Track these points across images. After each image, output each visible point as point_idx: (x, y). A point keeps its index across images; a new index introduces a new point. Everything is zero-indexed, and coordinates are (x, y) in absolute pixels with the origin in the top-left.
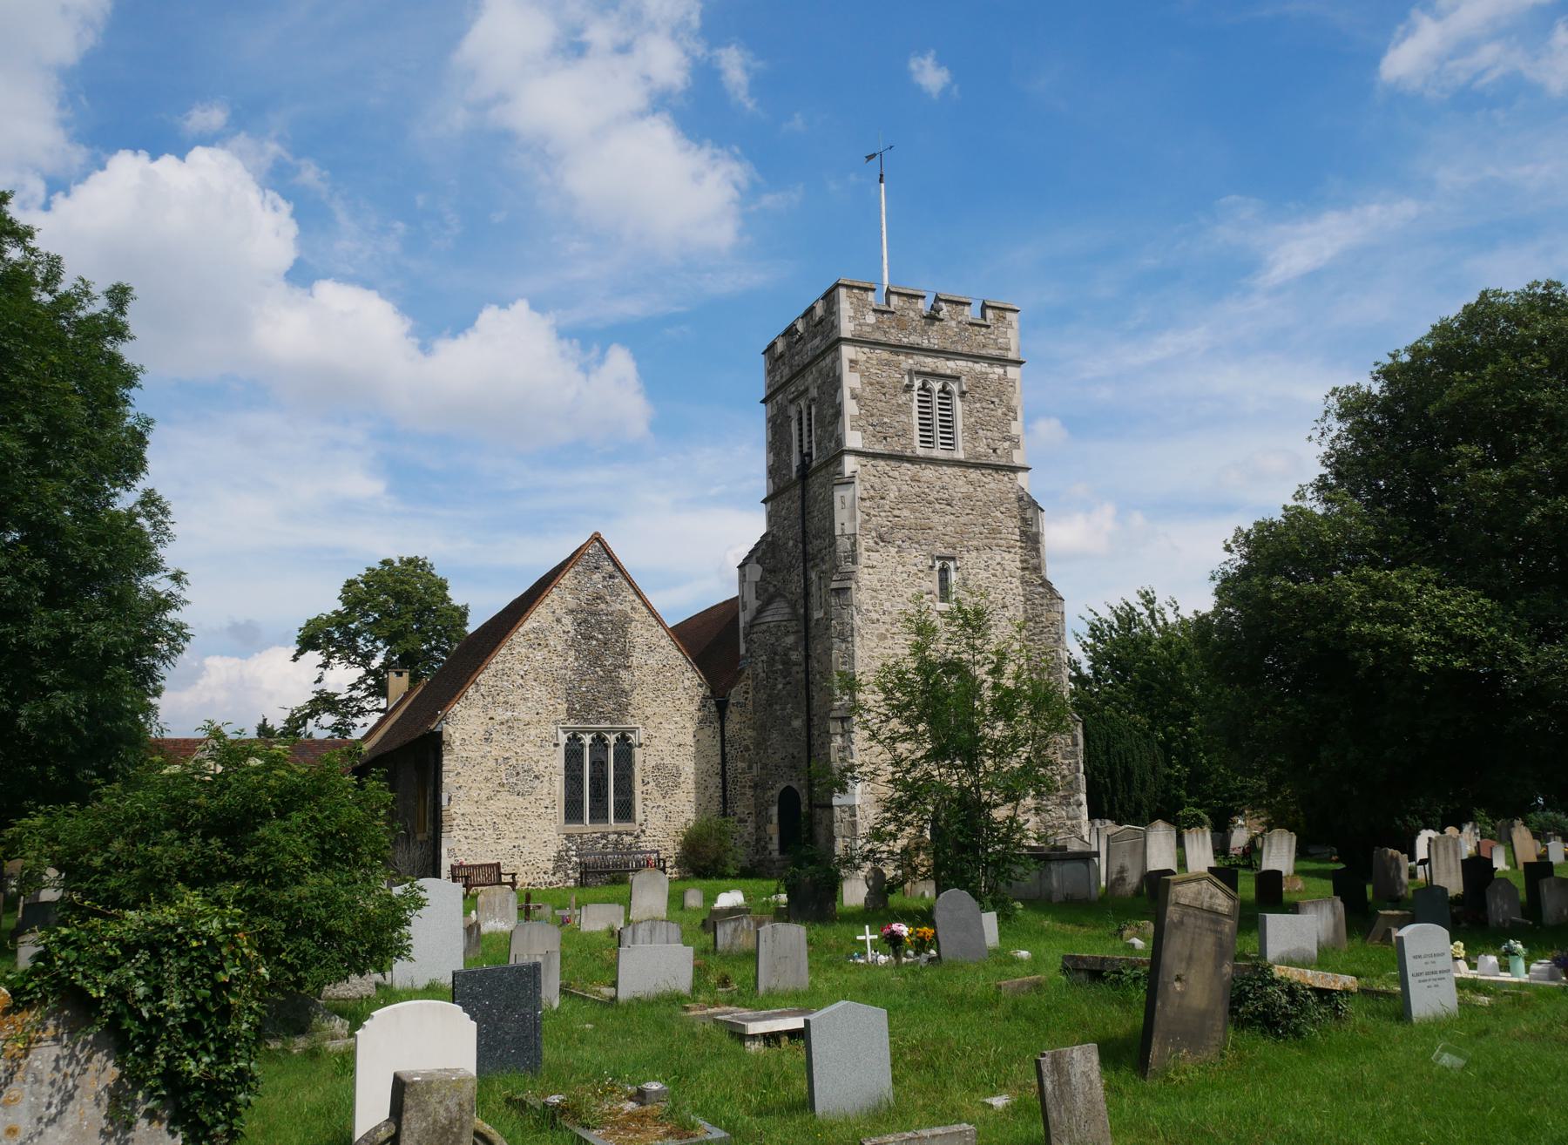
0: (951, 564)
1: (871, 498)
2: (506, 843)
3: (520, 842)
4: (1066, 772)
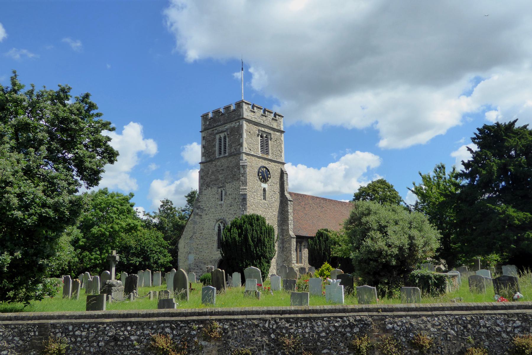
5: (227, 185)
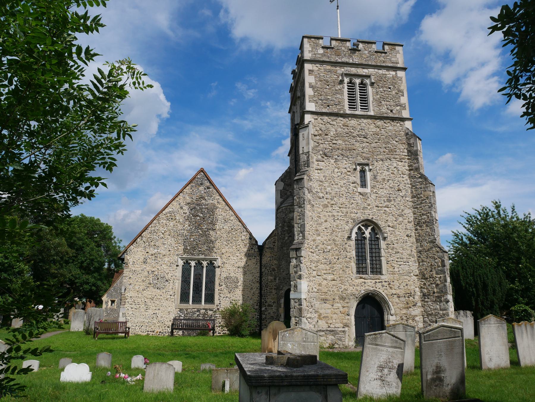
0: (367, 168)
1: (320, 135)
2: (150, 312)
3: (157, 311)
4: (438, 282)
5: (376, 163)
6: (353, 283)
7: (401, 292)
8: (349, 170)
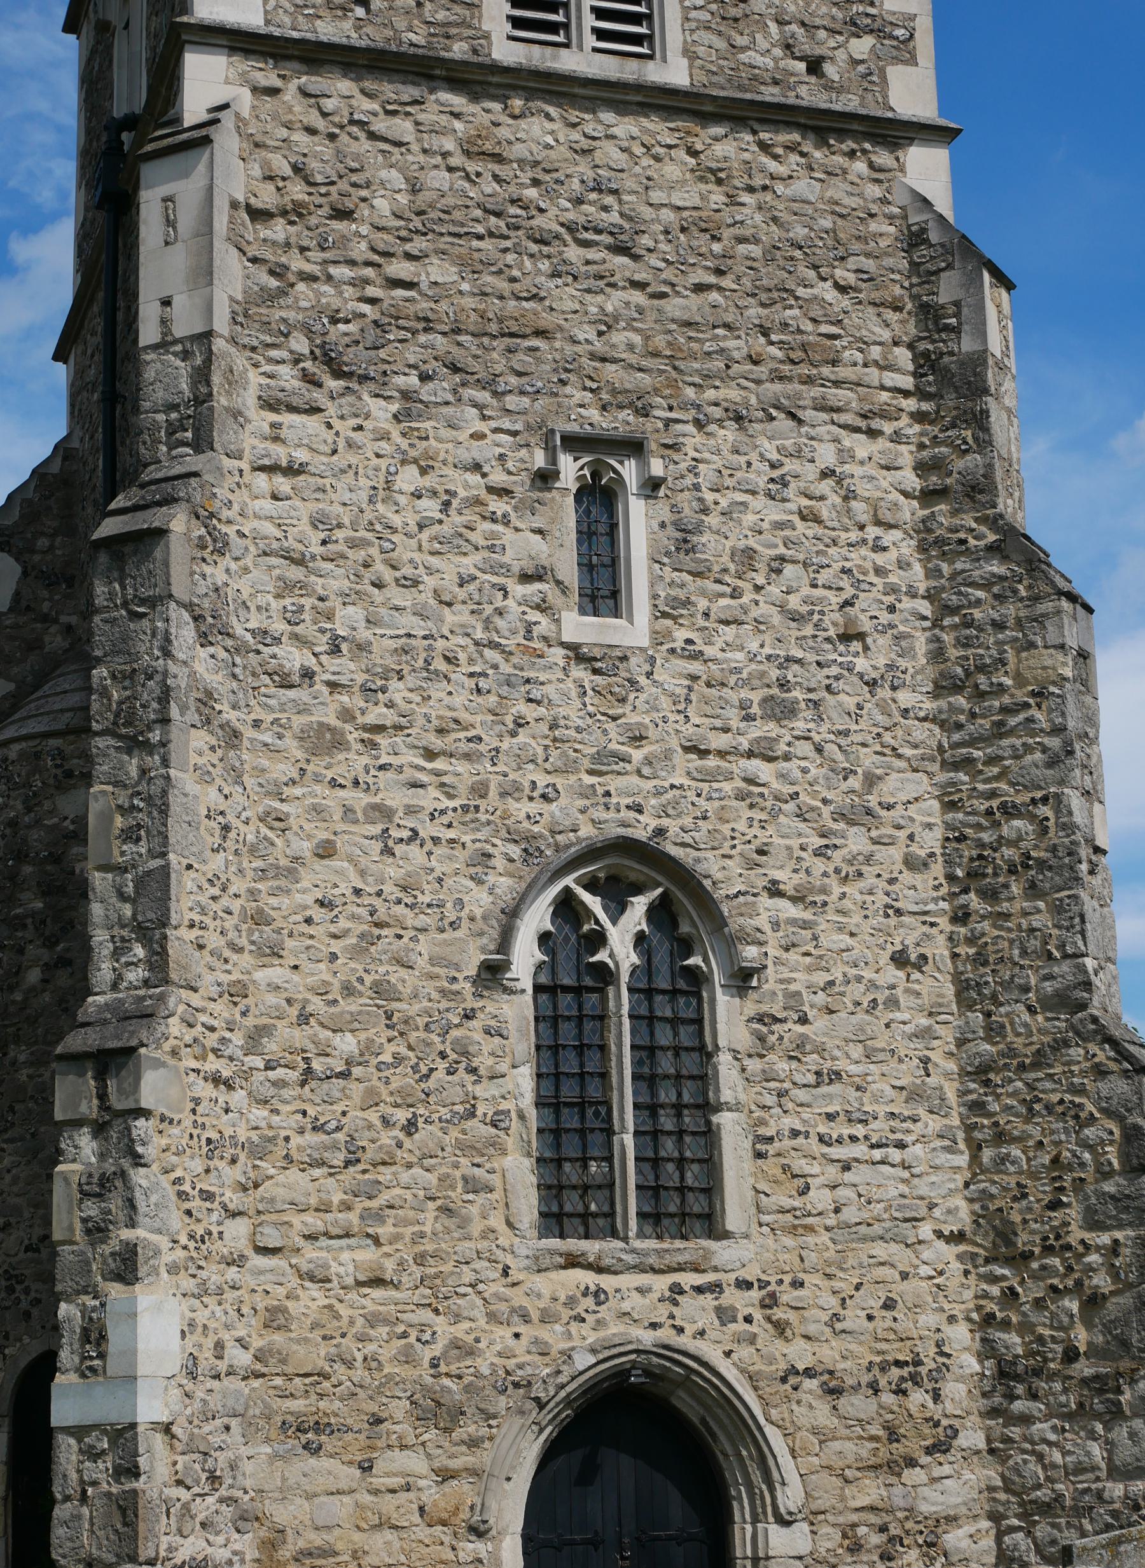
0: (629, 470)
1: (295, 213)
4: (1102, 1281)
5: (692, 439)
6: (518, 1298)
7: (848, 1356)
8: (498, 478)
